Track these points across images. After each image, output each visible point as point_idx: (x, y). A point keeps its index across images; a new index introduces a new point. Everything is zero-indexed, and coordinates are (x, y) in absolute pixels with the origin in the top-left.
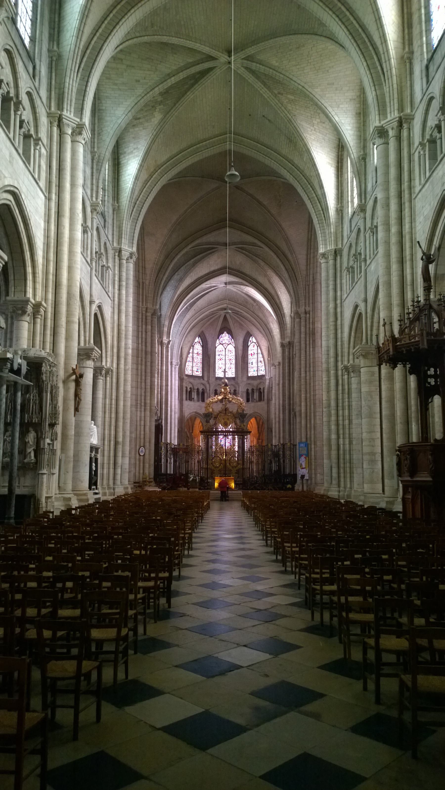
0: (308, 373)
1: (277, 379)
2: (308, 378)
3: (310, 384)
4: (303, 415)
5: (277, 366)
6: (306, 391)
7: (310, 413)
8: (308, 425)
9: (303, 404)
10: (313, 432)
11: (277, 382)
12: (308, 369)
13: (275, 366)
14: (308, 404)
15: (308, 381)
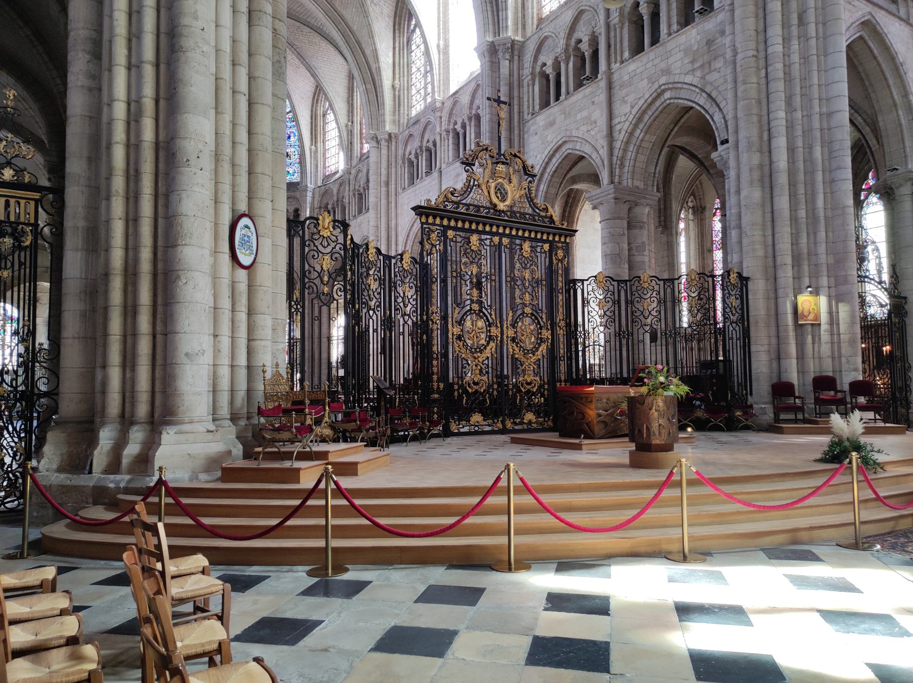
0: (795, 45)
1: (384, 172)
2: (795, 58)
3: (805, 78)
4: (782, 179)
5: (384, 143)
6: (789, 101)
7: (810, 173)
8: (802, 213)
9: (780, 143)
10: (822, 235)
11: (384, 178)
12: (795, 30)
13: (378, 142)
14: (800, 143)
15: (796, 70)
